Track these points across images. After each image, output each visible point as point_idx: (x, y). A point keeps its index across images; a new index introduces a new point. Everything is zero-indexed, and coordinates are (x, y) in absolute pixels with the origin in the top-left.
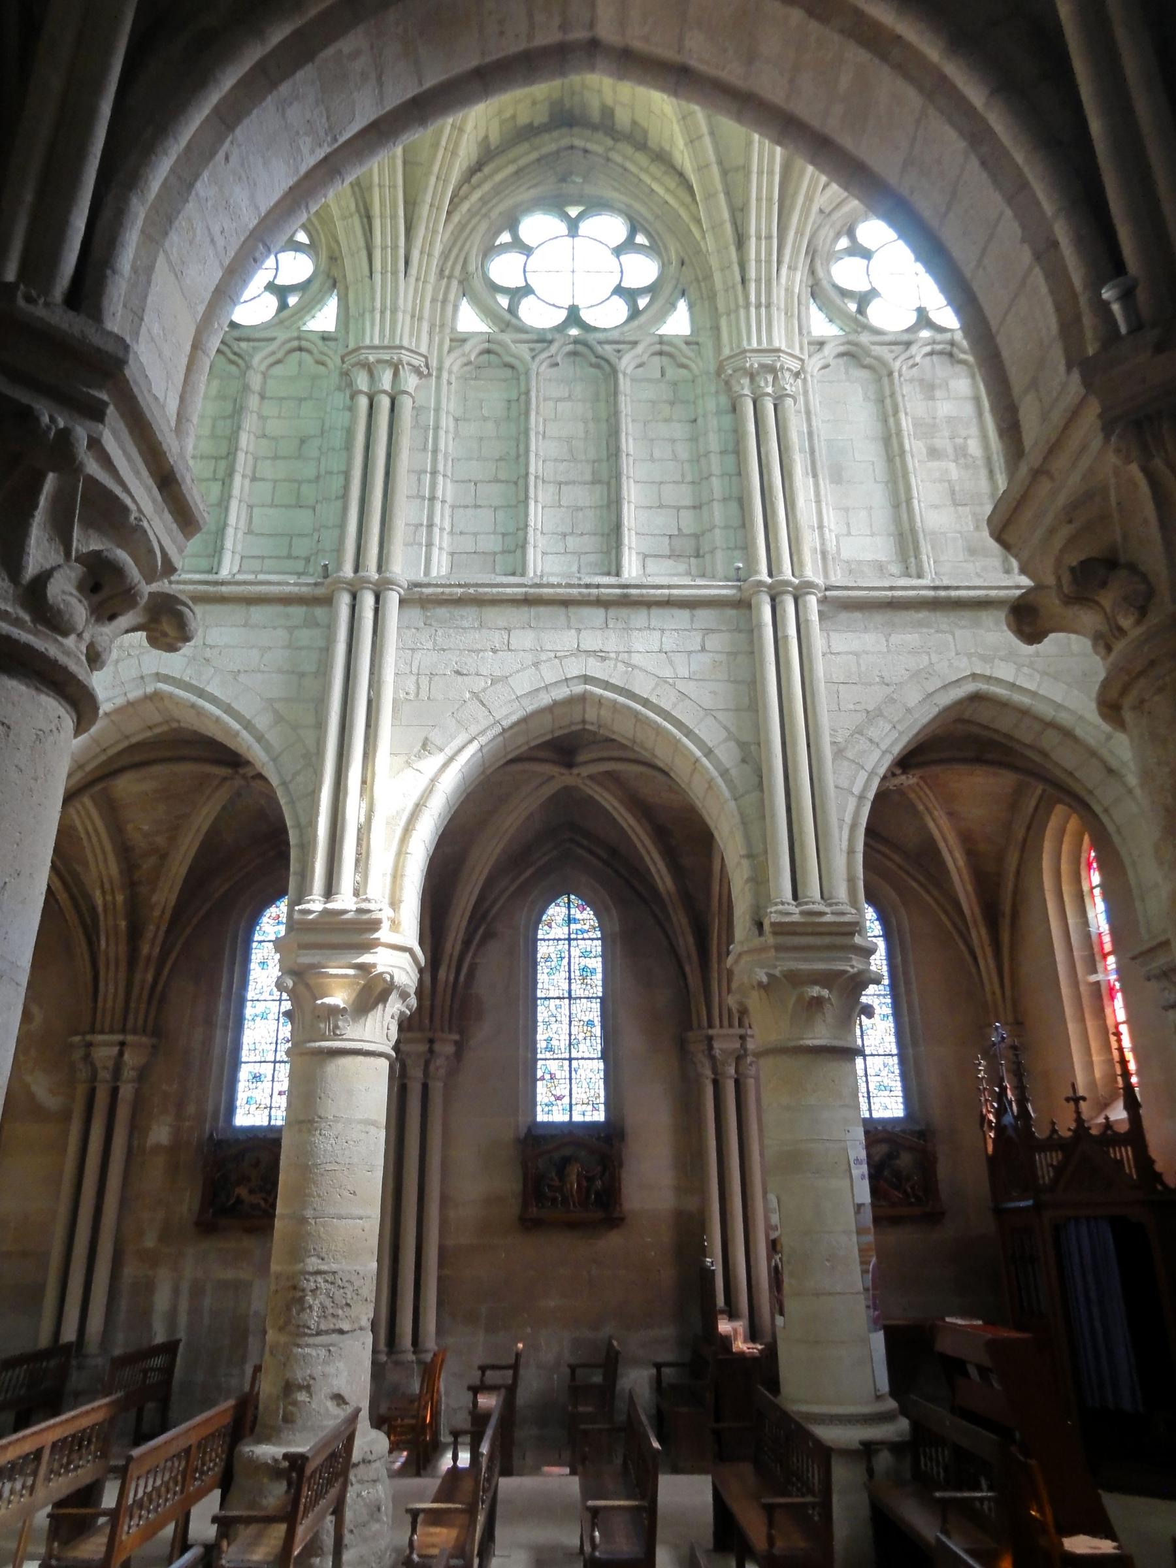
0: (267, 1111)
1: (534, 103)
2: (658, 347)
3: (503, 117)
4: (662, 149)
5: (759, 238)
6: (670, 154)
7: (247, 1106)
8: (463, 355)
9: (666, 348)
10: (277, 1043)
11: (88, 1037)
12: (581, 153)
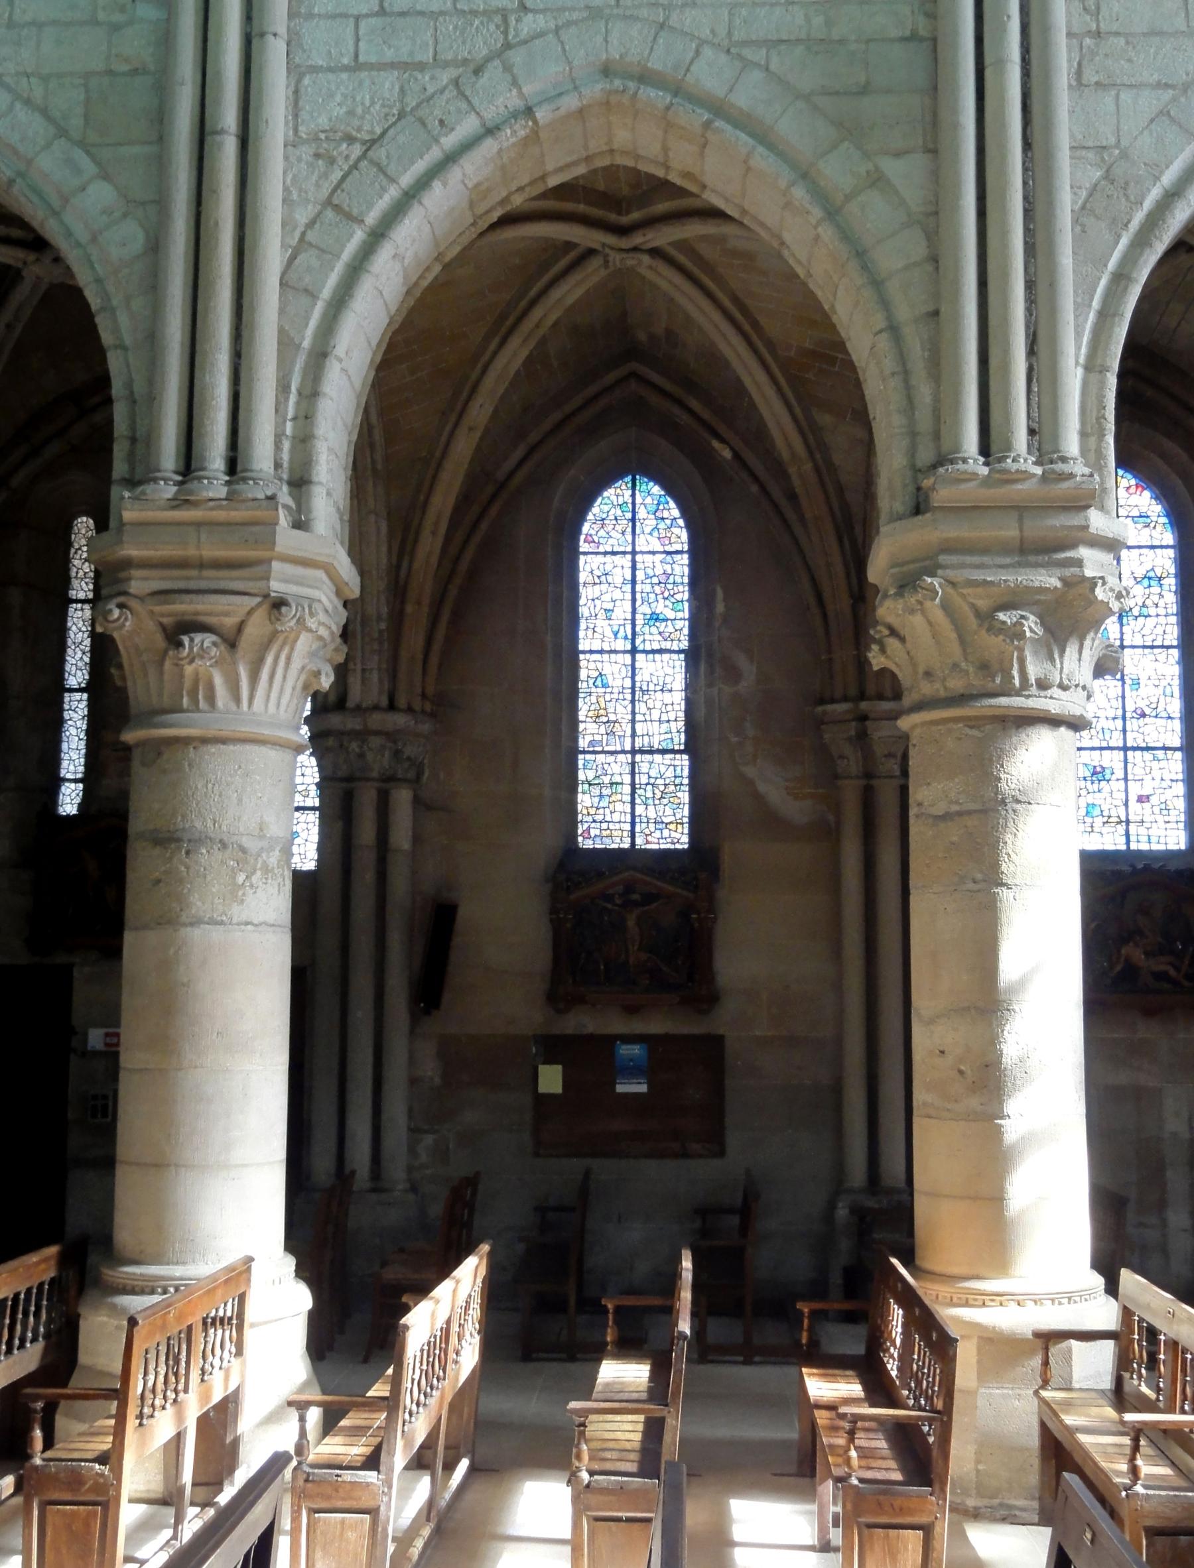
0: (1121, 829)
7: (1089, 820)
10: (1124, 718)
11: (864, 705)
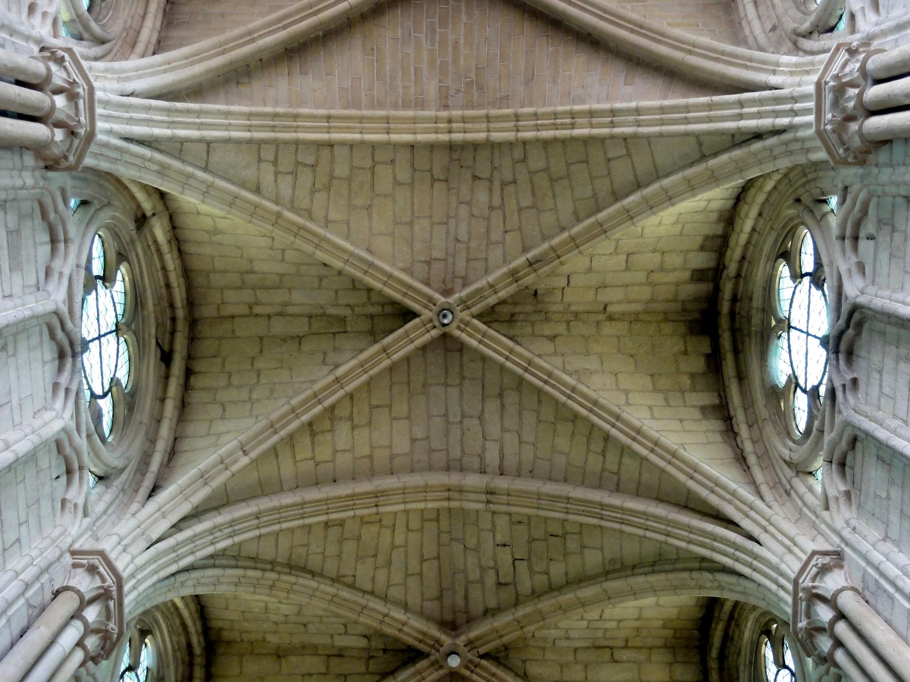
1: (685, 353)
2: (847, 242)
3: (688, 387)
4: (719, 219)
5: (741, 117)
6: (721, 212)
8: (837, 499)
9: (848, 232)
12: (738, 304)
